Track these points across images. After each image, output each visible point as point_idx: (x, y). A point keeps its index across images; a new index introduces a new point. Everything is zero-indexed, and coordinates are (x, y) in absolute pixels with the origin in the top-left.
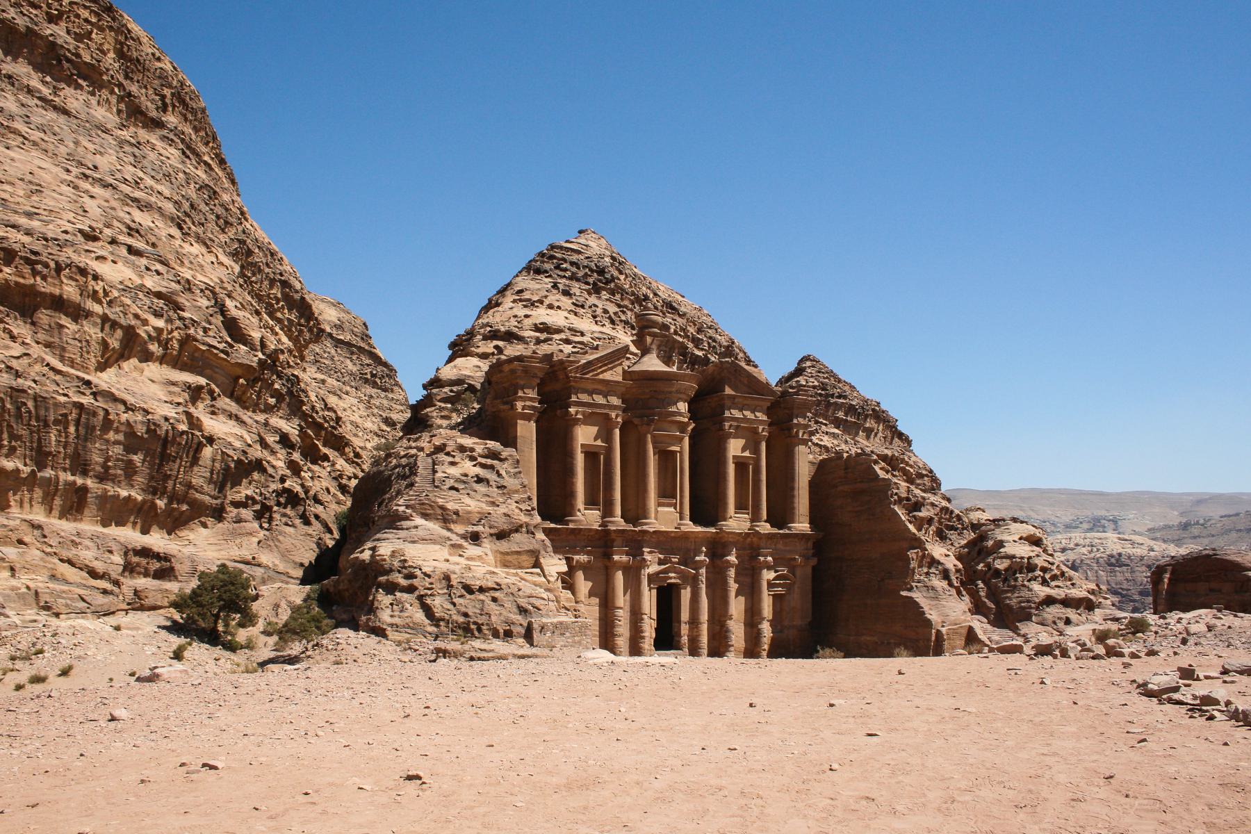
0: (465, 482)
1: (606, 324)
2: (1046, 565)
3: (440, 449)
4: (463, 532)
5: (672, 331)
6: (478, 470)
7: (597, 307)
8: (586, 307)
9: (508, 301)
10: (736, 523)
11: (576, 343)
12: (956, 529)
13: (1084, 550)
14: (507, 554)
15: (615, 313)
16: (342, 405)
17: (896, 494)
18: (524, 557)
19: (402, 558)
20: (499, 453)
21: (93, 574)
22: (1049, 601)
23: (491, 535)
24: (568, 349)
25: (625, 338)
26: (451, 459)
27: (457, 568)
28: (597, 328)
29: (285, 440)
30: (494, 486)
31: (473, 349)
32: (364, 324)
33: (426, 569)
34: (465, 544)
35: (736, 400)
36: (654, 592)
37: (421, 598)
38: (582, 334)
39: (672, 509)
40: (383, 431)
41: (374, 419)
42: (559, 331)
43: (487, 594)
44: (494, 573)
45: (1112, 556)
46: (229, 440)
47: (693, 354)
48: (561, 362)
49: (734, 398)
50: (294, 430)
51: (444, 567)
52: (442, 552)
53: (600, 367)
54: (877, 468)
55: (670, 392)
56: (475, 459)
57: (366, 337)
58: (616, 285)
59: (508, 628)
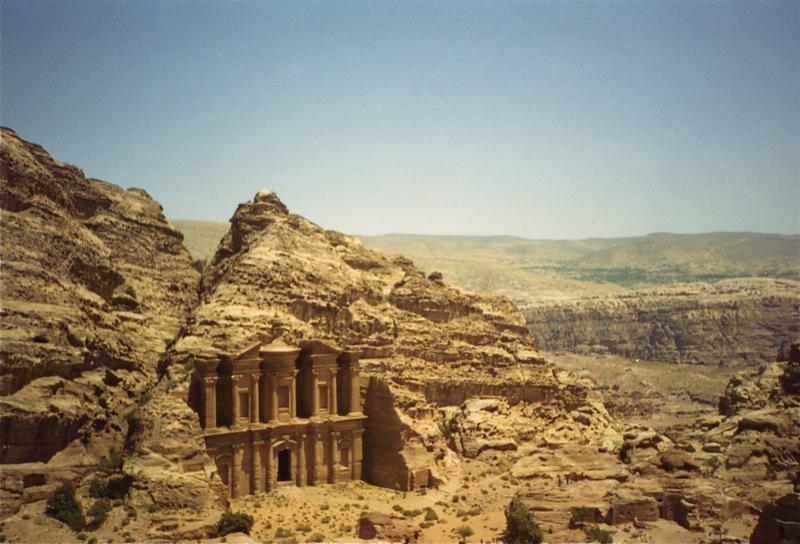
3: (165, 415)
6: (180, 426)
10: (319, 417)
13: (743, 293)
15: (272, 299)
21: (12, 491)
22: (486, 447)
28: (259, 313)
33: (153, 479)
34: (170, 463)
37: (150, 493)
38: (249, 320)
42: (237, 319)
45: (767, 299)
51: (160, 477)
52: (160, 469)
54: (390, 387)
57: (161, 218)
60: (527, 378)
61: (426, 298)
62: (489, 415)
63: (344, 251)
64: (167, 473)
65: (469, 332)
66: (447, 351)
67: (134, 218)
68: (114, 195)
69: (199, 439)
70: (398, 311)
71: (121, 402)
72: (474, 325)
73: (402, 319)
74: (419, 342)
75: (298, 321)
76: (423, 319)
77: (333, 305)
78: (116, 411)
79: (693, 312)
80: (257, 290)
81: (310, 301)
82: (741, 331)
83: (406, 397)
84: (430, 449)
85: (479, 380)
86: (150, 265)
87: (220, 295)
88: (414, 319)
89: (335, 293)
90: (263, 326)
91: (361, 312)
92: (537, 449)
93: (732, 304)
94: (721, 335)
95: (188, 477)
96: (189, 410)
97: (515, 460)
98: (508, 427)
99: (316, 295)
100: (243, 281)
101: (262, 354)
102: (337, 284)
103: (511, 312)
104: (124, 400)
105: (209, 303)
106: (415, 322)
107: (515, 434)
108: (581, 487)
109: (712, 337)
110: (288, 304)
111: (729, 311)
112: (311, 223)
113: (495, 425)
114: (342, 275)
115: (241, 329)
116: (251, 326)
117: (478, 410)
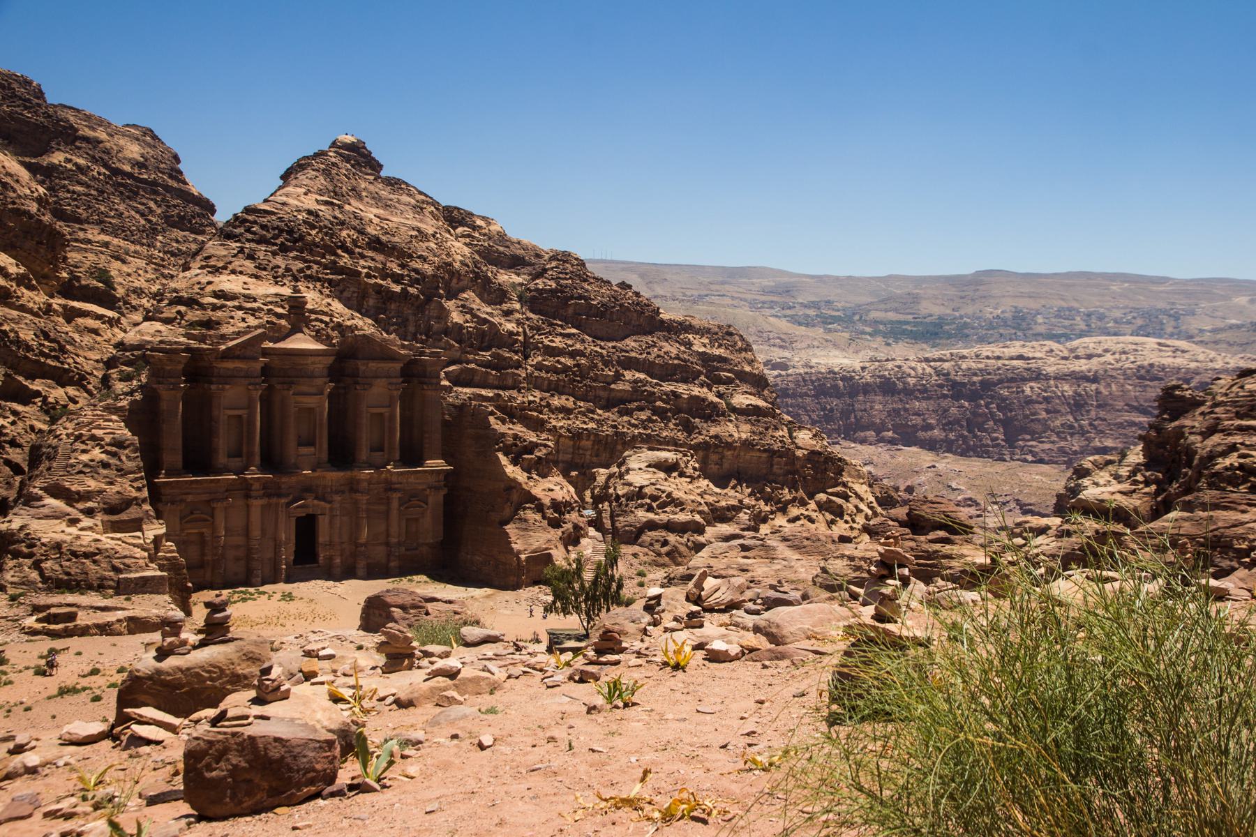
0: (91, 467)
1: (287, 283)
3: (78, 438)
6: (104, 456)
7: (279, 267)
8: (269, 268)
15: (301, 271)
22: (651, 525)
26: (84, 447)
27: (68, 538)
33: (44, 540)
38: (255, 300)
42: (234, 297)
44: (98, 540)
51: (59, 537)
54: (492, 419)
57: (176, 174)
60: (744, 436)
61: (580, 297)
62: (662, 475)
63: (469, 236)
64: (73, 530)
65: (651, 358)
66: (613, 386)
67: (127, 168)
68: (94, 130)
69: (136, 480)
70: (532, 316)
71: (32, 428)
73: (538, 329)
74: (566, 369)
75: (348, 312)
76: (574, 331)
77: (412, 290)
78: (19, 440)
79: (1032, 384)
80: (274, 254)
81: (372, 281)
82: (1102, 414)
83: (516, 437)
84: (555, 524)
85: (664, 434)
87: (209, 257)
88: (559, 330)
90: (280, 310)
91: (466, 310)
92: (738, 531)
94: (1072, 419)
95: (108, 541)
96: (125, 433)
97: (698, 547)
98: (693, 498)
99: (384, 274)
100: (249, 236)
101: (266, 353)
102: (424, 259)
103: (740, 350)
104: (39, 425)
105: (189, 268)
106: (561, 334)
107: (706, 509)
108: (779, 567)
109: (1058, 423)
110: (330, 282)
112: (421, 193)
113: (669, 489)
114: (434, 246)
115: (240, 313)
116: (260, 309)
117: (643, 465)
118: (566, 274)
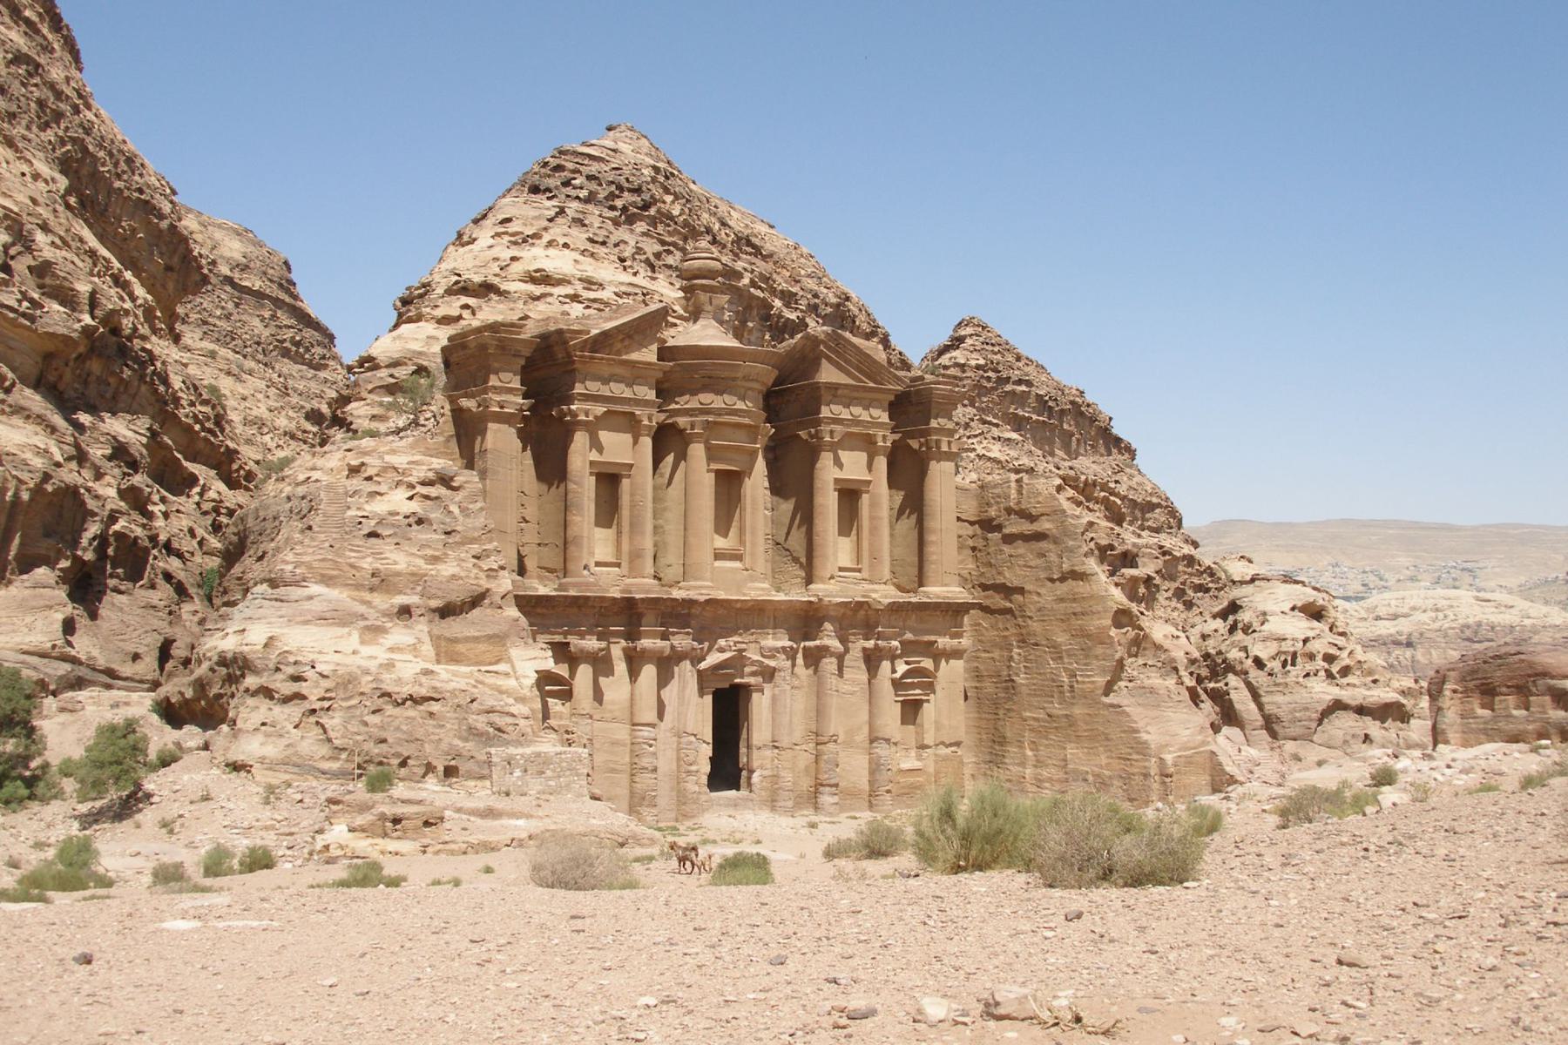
0: (393, 525)
1: (641, 271)
2: (1333, 651)
3: (354, 471)
4: (387, 606)
5: (746, 281)
7: (626, 243)
8: (610, 244)
9: (484, 235)
11: (589, 300)
12: (1207, 590)
13: (1425, 617)
14: (455, 641)
15: (658, 255)
16: (241, 391)
17: (1092, 539)
18: (482, 647)
19: (286, 648)
20: (452, 479)
22: (1338, 706)
23: (434, 610)
24: (576, 310)
25: (668, 291)
27: (373, 665)
28: (626, 278)
29: (120, 452)
30: (439, 531)
31: (428, 310)
32: (286, 263)
33: (319, 668)
34: (390, 625)
35: (840, 392)
36: (709, 699)
38: (601, 286)
39: (737, 564)
40: (305, 432)
41: (291, 413)
43: (421, 708)
45: (1468, 627)
46: (23, 456)
47: (780, 316)
48: (560, 332)
49: (836, 389)
50: (139, 438)
53: (622, 340)
55: (734, 379)
56: (414, 487)
57: (288, 285)
58: (658, 211)
59: (453, 763)
72: (1131, 477)
76: (1014, 436)
86: (260, 357)
87: (508, 220)
88: (996, 432)
89: (816, 296)
93: (1403, 638)
111: (1398, 652)
116: (607, 304)
117: (1287, 608)
118: (993, 345)
